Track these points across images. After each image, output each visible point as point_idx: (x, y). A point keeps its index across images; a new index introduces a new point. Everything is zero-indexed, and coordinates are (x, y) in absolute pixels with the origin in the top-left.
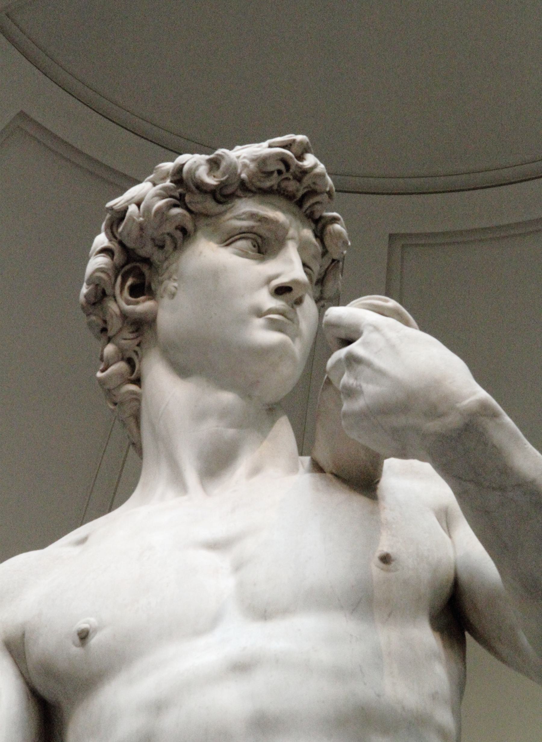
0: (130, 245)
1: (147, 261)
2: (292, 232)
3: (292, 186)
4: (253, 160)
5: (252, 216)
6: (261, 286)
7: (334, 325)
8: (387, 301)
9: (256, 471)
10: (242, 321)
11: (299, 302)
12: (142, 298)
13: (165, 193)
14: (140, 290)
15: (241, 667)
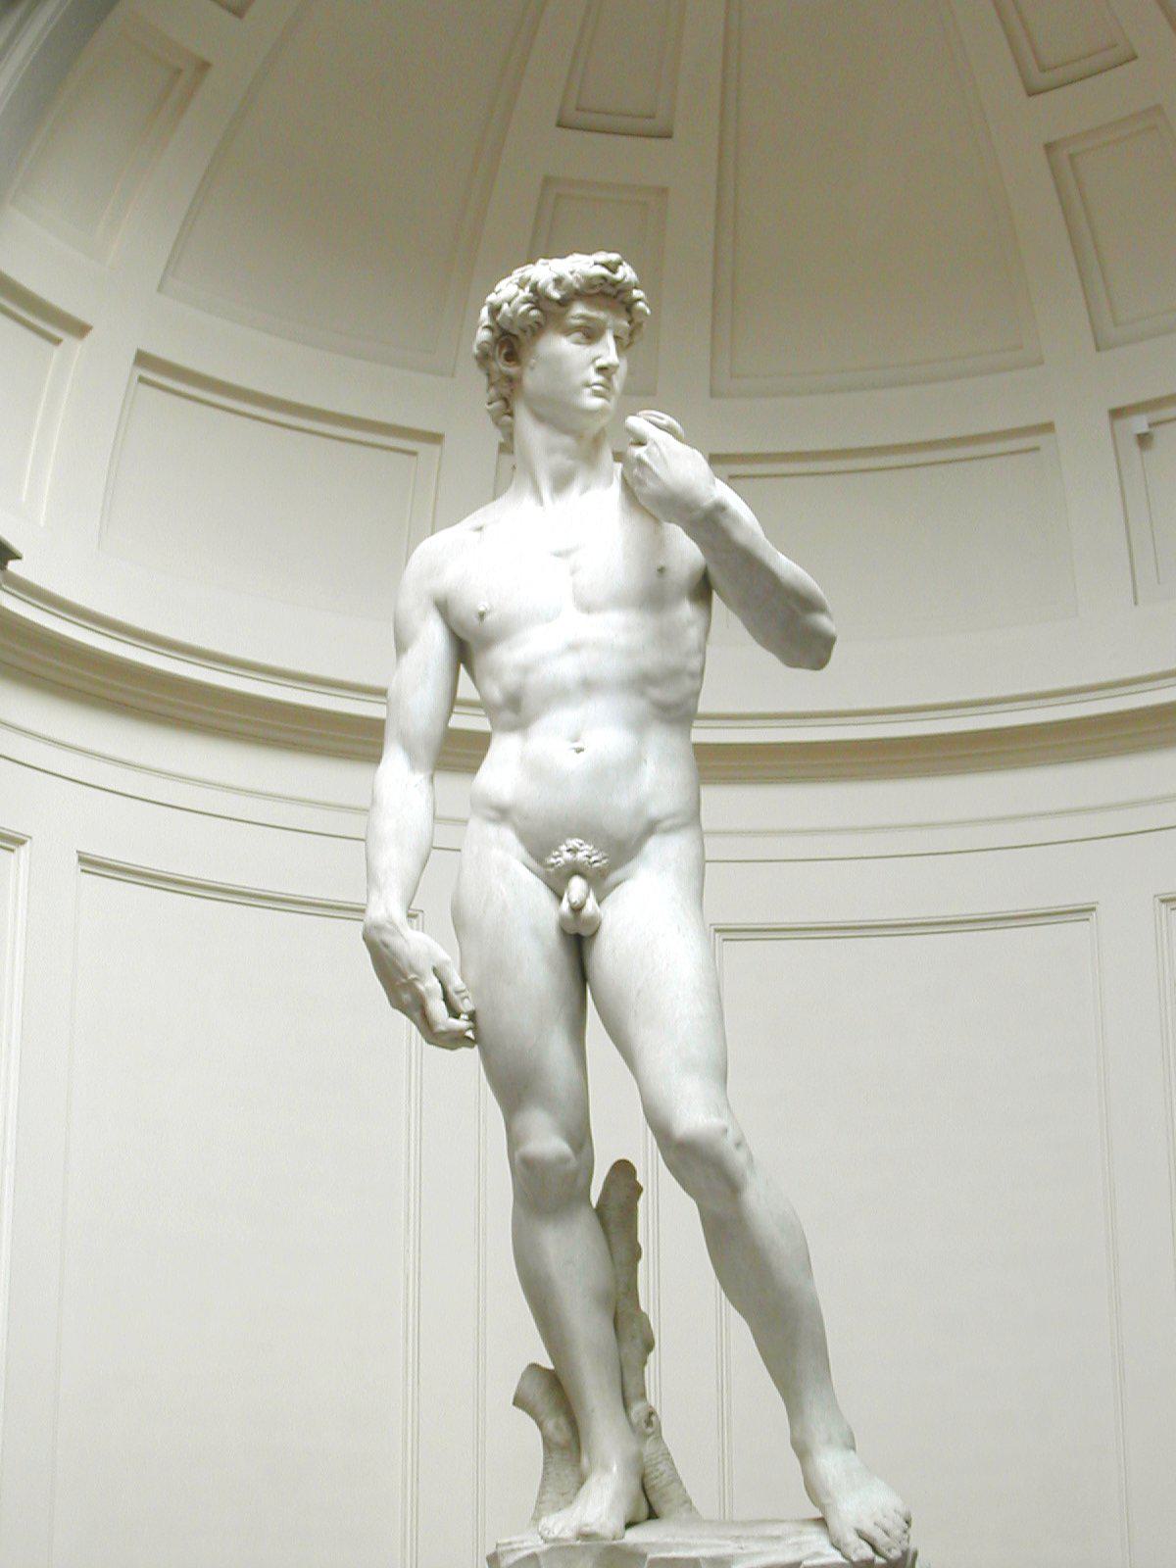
0: (504, 327)
1: (515, 336)
2: (610, 323)
3: (610, 290)
4: (585, 277)
5: (582, 317)
6: (588, 365)
7: (631, 432)
8: (662, 419)
9: (586, 489)
10: (577, 391)
11: (615, 372)
12: (513, 363)
13: (527, 301)
14: (512, 356)
15: (574, 648)
